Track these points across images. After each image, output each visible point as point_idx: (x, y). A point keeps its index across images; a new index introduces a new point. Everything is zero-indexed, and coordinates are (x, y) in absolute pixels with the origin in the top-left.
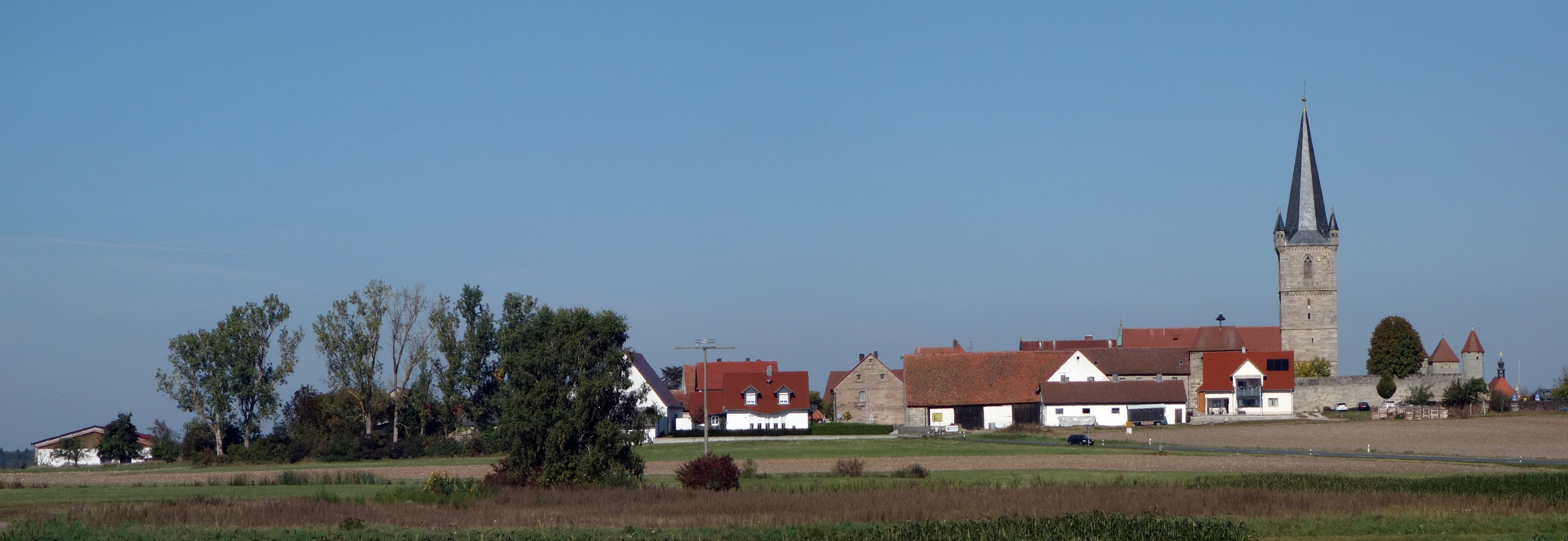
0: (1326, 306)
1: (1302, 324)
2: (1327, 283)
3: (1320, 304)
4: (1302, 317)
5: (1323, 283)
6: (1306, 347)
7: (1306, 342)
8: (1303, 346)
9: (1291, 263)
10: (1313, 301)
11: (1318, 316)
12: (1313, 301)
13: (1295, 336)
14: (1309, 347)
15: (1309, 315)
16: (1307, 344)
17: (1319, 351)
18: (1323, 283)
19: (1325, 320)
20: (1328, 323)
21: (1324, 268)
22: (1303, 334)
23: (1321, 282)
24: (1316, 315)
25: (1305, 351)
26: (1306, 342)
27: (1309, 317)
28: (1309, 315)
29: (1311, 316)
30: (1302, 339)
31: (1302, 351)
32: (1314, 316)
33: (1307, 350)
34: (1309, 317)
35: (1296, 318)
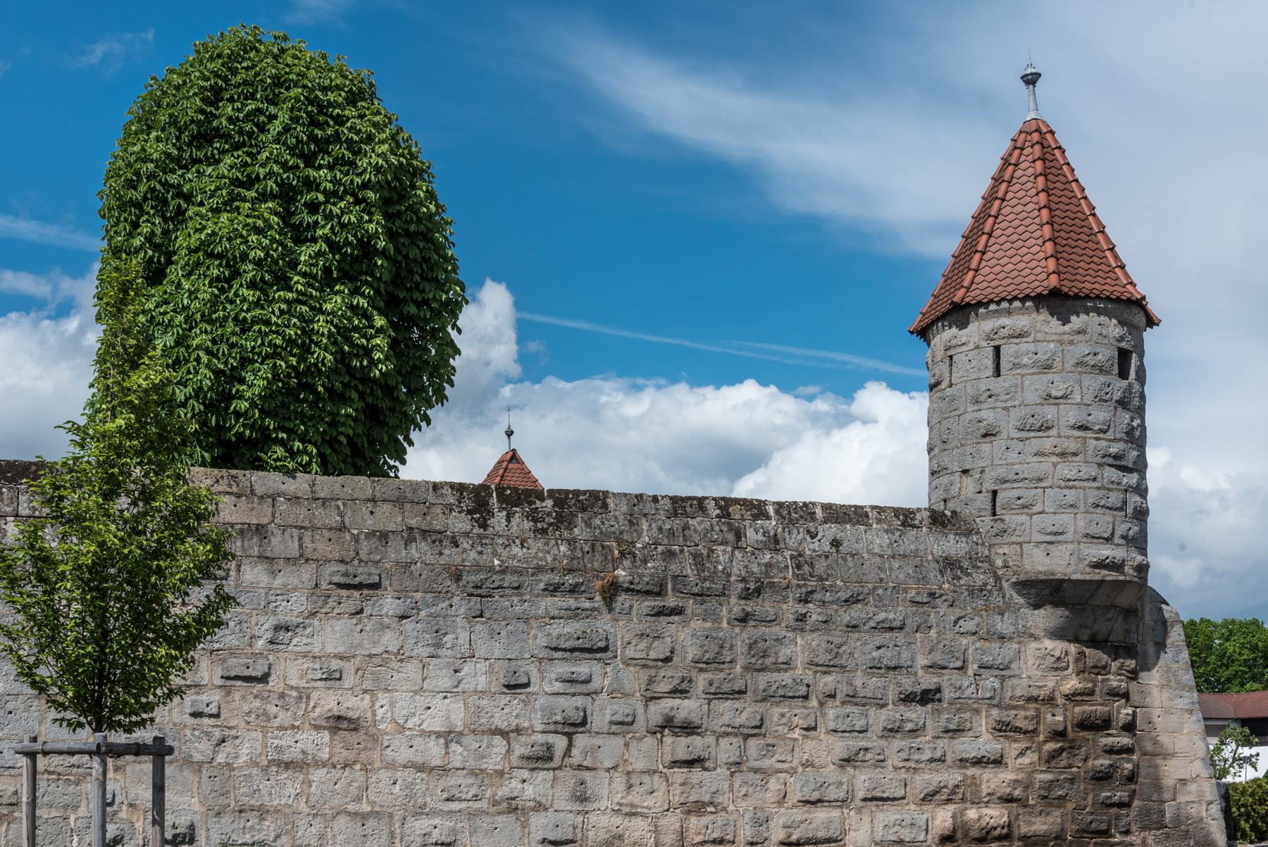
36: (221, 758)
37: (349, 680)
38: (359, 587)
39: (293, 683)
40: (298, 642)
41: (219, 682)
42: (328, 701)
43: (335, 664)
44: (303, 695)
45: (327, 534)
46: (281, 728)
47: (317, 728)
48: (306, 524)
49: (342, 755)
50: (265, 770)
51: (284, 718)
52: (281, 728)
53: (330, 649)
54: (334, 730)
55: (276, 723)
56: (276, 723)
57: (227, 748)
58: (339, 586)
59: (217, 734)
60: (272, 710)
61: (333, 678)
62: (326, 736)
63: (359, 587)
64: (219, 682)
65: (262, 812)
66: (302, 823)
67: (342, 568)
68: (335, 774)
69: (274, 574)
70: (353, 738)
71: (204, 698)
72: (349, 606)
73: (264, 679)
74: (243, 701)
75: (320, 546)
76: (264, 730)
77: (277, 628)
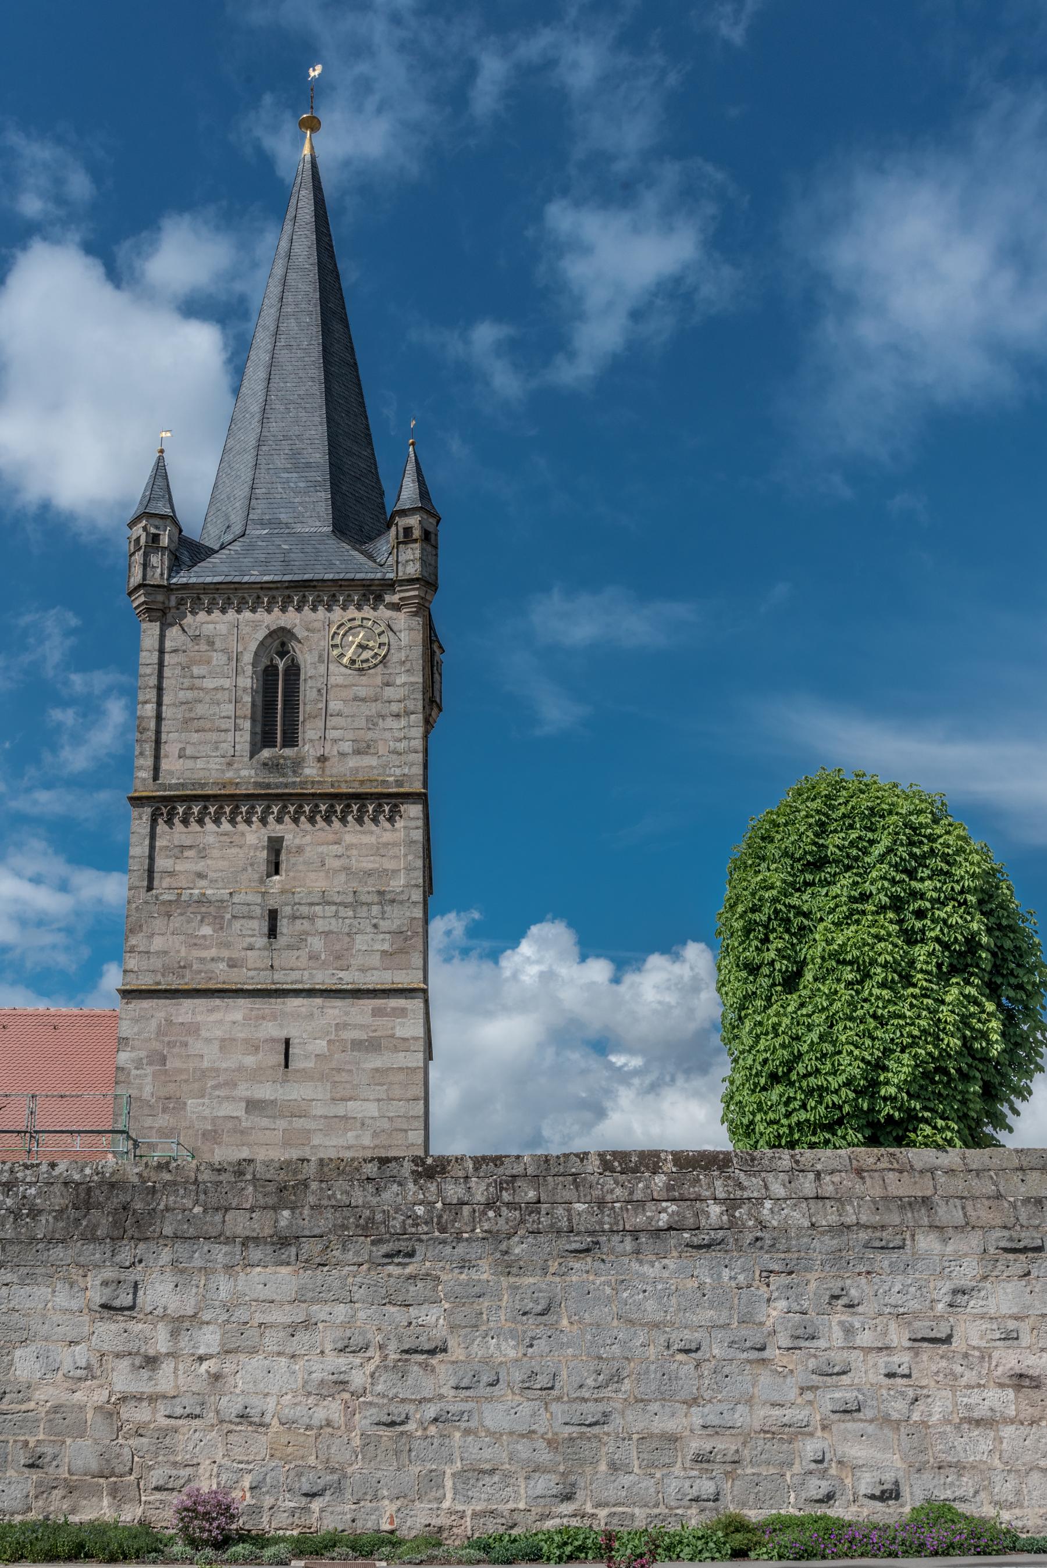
0: (369, 873)
1: (232, 964)
2: (371, 761)
3: (337, 864)
4: (237, 925)
5: (353, 762)
6: (243, 1090)
7: (250, 1061)
8: (232, 1084)
9: (196, 670)
10: (300, 850)
11: (321, 925)
12: (300, 850)
13: (193, 1029)
14: (265, 1091)
15: (273, 916)
16: (255, 1075)
17: (318, 1110)
18: (353, 762)
19: (361, 942)
20: (376, 960)
21: (362, 692)
22: (238, 1016)
23: (342, 755)
24: (311, 918)
25: (241, 1113)
26: (250, 1061)
27: (272, 932)
28: (273, 916)
29: (284, 926)
30: (226, 1044)
31: (227, 1109)
32: (300, 925)
33: (253, 1106)
34: (272, 932)
35: (206, 930)
36: (916, 1417)
37: (1026, 1339)
38: (1024, 1250)
39: (974, 1343)
40: (975, 1304)
41: (908, 1344)
42: (1009, 1360)
43: (1011, 1324)
44: (985, 1355)
45: (986, 1203)
46: (969, 1387)
47: (1001, 1386)
48: (966, 1194)
49: (1028, 1412)
50: (958, 1427)
51: (970, 1377)
52: (969, 1387)
53: (1004, 1310)
54: (1018, 1388)
55: (963, 1381)
56: (963, 1381)
57: (921, 1406)
58: (1006, 1250)
59: (911, 1393)
60: (959, 1369)
61: (1010, 1337)
62: (1011, 1394)
63: (1024, 1250)
64: (908, 1344)
65: (960, 1468)
66: (998, 1479)
67: (1006, 1233)
68: (1024, 1430)
69: (945, 1241)
70: (1036, 1395)
71: (896, 1359)
72: (1017, 1269)
73: (947, 1340)
74: (931, 1361)
75: (980, 1213)
76: (953, 1389)
77: (955, 1292)
